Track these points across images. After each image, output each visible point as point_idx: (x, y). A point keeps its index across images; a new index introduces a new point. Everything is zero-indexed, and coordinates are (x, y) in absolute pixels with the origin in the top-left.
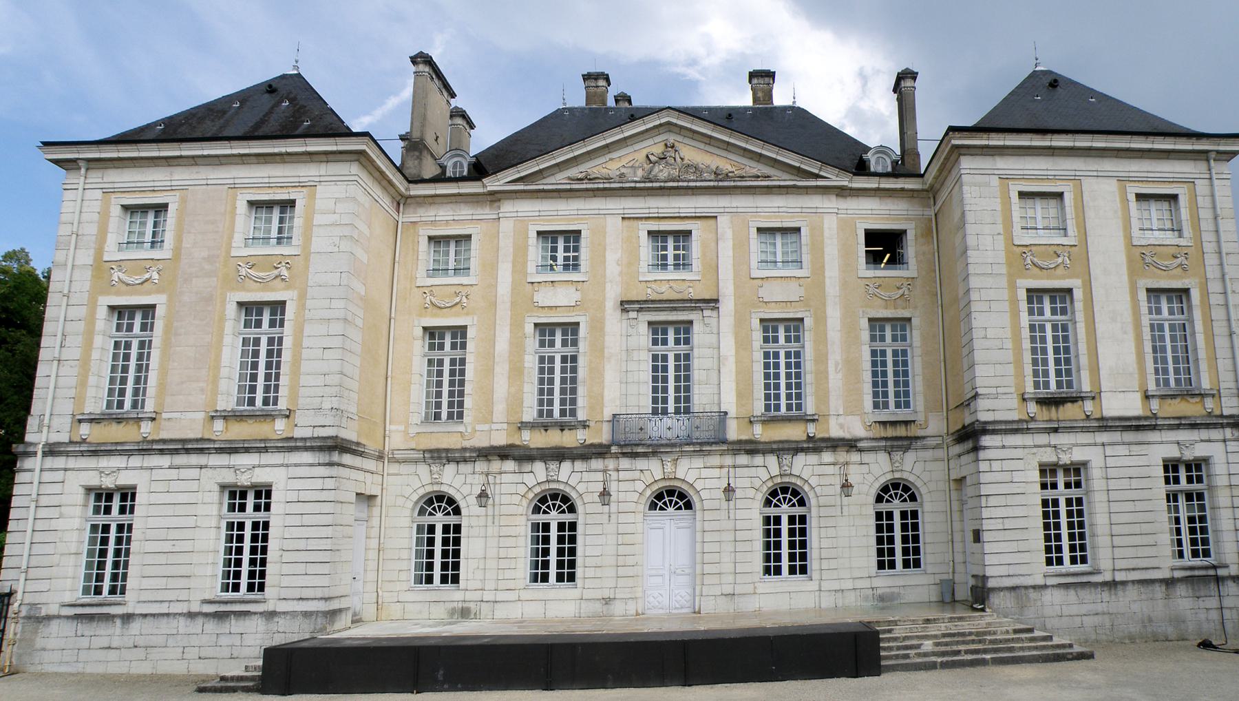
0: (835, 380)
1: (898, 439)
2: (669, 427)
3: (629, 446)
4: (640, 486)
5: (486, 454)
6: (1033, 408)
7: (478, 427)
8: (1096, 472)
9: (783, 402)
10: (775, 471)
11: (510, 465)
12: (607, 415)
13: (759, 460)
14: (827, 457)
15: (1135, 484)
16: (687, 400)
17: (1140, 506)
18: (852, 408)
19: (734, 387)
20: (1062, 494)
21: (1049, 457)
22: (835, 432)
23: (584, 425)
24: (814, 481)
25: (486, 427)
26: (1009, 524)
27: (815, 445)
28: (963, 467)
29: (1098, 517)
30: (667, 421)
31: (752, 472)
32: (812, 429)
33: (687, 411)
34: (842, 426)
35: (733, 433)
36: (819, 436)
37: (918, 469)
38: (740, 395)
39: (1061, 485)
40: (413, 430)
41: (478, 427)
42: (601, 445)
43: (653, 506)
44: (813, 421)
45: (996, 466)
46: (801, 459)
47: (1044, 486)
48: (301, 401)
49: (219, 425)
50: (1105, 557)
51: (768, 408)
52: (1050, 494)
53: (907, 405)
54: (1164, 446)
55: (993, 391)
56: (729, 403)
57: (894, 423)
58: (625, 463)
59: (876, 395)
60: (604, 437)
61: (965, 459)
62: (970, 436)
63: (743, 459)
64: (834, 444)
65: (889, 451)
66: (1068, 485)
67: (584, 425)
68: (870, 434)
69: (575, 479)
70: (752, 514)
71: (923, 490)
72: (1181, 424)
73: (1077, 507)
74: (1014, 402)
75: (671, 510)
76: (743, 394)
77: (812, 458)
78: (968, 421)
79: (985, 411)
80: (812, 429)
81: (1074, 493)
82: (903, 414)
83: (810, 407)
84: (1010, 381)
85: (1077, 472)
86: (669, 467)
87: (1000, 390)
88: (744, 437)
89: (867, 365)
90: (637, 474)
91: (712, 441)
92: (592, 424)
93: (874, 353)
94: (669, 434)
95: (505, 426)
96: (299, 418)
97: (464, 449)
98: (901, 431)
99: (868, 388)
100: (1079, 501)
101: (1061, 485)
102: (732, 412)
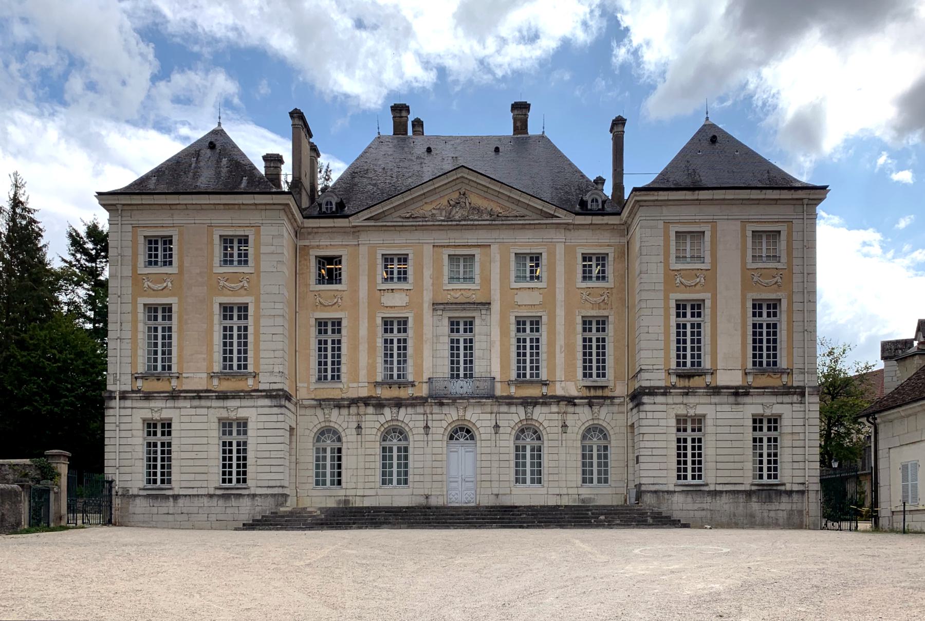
0: (560, 358)
1: (596, 398)
2: (461, 387)
3: (440, 399)
4: (445, 424)
5: (354, 402)
6: (674, 379)
7: (351, 385)
8: (709, 422)
9: (528, 372)
10: (523, 417)
11: (370, 410)
12: (425, 379)
13: (513, 409)
14: (554, 408)
15: (733, 430)
16: (471, 369)
17: (735, 444)
18: (569, 377)
19: (499, 360)
20: (689, 435)
21: (682, 411)
22: (559, 392)
23: (413, 385)
24: (546, 424)
25: (355, 385)
26: (655, 452)
27: (546, 401)
28: (633, 417)
29: (709, 451)
30: (461, 383)
31: (509, 416)
32: (545, 390)
33: (471, 376)
34: (563, 389)
35: (498, 393)
36: (549, 394)
37: (608, 418)
38: (502, 367)
39: (689, 430)
40: (312, 387)
41: (351, 385)
42: (421, 398)
43: (451, 438)
44: (546, 385)
45: (650, 415)
46: (538, 410)
47: (679, 430)
48: (261, 367)
49: (216, 382)
50: (711, 477)
51: (519, 375)
52: (682, 435)
53: (604, 376)
54: (753, 407)
55: (651, 367)
56: (496, 372)
57: (595, 388)
58: (436, 409)
59: (585, 368)
60: (424, 391)
61: (635, 411)
62: (637, 397)
63: (504, 409)
64: (559, 399)
65: (590, 405)
66: (693, 430)
67: (413, 385)
68: (580, 394)
69: (409, 418)
70: (508, 443)
71: (611, 432)
72: (765, 390)
73: (698, 443)
74: (662, 375)
75: (462, 440)
76: (504, 366)
77: (545, 409)
78: (636, 387)
79: (647, 380)
80: (545, 390)
81: (696, 435)
82: (601, 382)
83: (544, 376)
84: (662, 361)
85: (700, 421)
86: (461, 413)
87: (655, 367)
88: (505, 394)
89: (580, 348)
90: (443, 416)
91: (487, 397)
92: (416, 384)
93: (584, 340)
94: (461, 391)
95: (366, 384)
96: (262, 378)
97: (343, 399)
98: (599, 393)
99: (580, 364)
100: (700, 440)
101: (689, 430)
102: (498, 379)
